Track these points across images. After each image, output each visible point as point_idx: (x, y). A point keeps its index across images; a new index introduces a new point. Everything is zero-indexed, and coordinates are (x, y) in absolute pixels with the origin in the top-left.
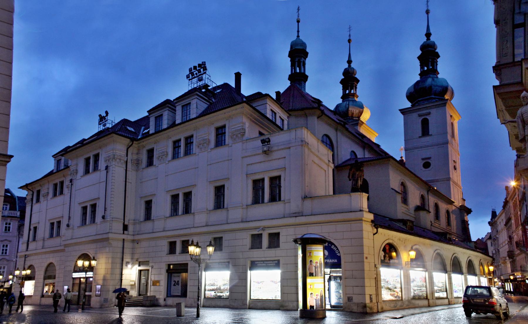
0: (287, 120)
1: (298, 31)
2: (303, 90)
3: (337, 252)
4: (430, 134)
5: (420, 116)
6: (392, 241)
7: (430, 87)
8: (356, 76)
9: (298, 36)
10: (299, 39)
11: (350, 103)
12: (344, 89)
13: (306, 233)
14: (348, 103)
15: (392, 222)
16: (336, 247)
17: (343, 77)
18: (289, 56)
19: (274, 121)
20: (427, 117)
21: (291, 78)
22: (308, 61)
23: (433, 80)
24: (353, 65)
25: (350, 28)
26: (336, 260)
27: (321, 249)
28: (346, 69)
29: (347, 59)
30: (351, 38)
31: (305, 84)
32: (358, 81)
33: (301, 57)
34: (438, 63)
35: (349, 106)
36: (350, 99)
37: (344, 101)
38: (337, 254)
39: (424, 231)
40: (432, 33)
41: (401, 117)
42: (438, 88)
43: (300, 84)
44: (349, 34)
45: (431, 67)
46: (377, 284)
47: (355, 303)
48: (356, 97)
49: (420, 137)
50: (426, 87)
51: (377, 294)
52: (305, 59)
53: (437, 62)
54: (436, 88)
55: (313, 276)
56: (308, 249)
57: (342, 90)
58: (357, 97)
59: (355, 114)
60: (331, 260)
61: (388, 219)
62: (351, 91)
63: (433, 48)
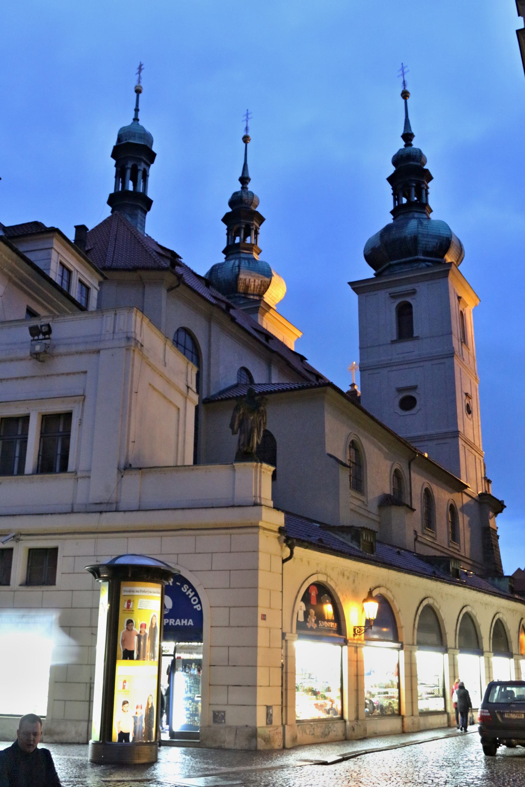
0: (98, 288)
1: (137, 110)
2: (138, 229)
3: (195, 600)
4: (415, 335)
5: (393, 296)
6: (325, 576)
7: (415, 239)
8: (257, 209)
9: (136, 119)
10: (138, 124)
12: (231, 233)
13: (122, 554)
14: (237, 262)
15: (328, 532)
16: (194, 590)
17: (229, 210)
18: (113, 156)
19: (65, 288)
20: (409, 299)
21: (112, 200)
22: (153, 170)
23: (420, 223)
24: (250, 187)
25: (247, 114)
26: (191, 620)
27: (158, 593)
28: (235, 194)
29: (240, 175)
30: (250, 134)
31: (145, 218)
32: (261, 220)
33: (141, 160)
34: (429, 190)
35: (239, 269)
36: (242, 255)
37: (228, 258)
38: (195, 607)
39: (399, 553)
40: (415, 134)
41: (354, 297)
42: (430, 240)
43: (134, 216)
44: (245, 126)
45: (416, 199)
46: (286, 681)
47: (230, 727)
48: (256, 252)
49: (393, 342)
50: (405, 237)
51: (284, 705)
52: (149, 166)
53: (428, 188)
54: (426, 239)
55: (132, 658)
56: (125, 591)
57: (226, 237)
58: (259, 252)
59: (252, 287)
60: (178, 620)
61: (318, 525)
62: (245, 239)
63: (417, 161)
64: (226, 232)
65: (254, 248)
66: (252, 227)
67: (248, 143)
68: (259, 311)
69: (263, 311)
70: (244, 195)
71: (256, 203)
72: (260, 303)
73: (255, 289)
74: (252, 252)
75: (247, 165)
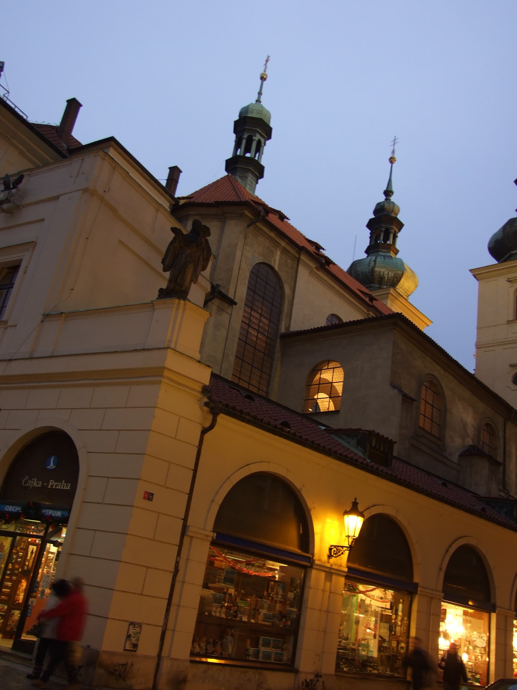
11: (378, 260)
12: (374, 237)
14: (374, 258)
17: (373, 217)
24: (393, 199)
25: (395, 140)
29: (385, 188)
30: (396, 156)
35: (375, 263)
36: (381, 253)
41: (475, 284)
44: (392, 149)
48: (393, 252)
49: (509, 322)
57: (369, 239)
58: (397, 252)
59: (386, 278)
64: (369, 235)
65: (392, 248)
66: (391, 231)
67: (394, 163)
68: (389, 298)
69: (393, 298)
70: (386, 204)
71: (397, 212)
72: (390, 290)
73: (389, 281)
74: (389, 251)
75: (391, 183)
